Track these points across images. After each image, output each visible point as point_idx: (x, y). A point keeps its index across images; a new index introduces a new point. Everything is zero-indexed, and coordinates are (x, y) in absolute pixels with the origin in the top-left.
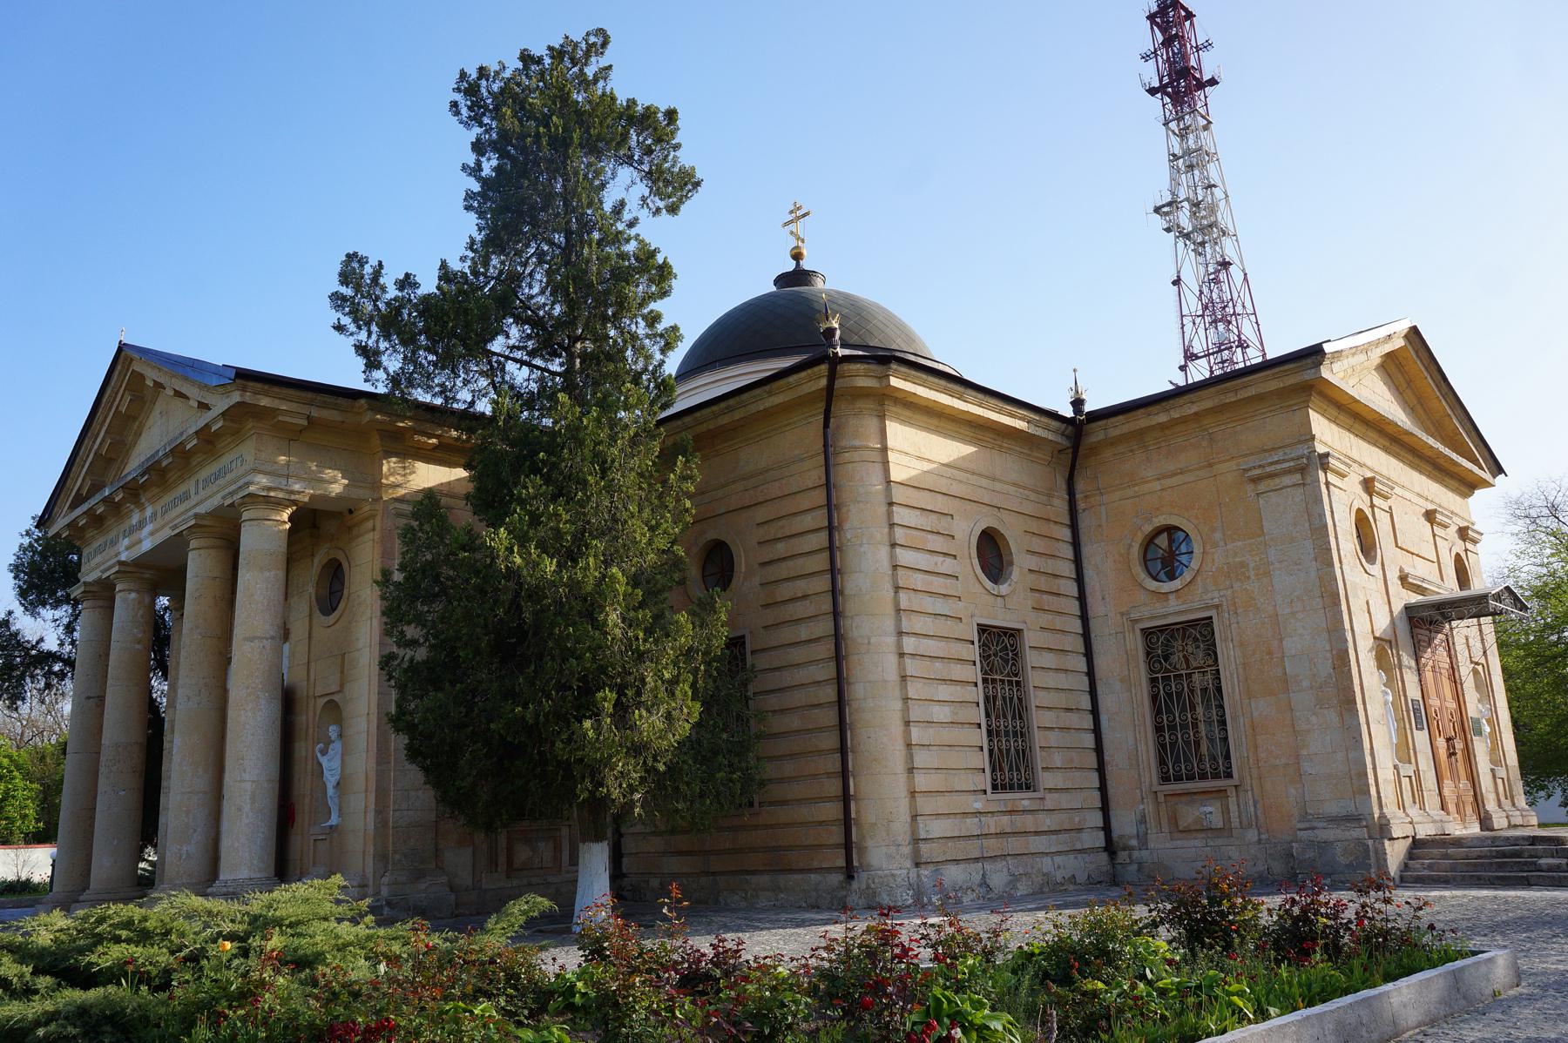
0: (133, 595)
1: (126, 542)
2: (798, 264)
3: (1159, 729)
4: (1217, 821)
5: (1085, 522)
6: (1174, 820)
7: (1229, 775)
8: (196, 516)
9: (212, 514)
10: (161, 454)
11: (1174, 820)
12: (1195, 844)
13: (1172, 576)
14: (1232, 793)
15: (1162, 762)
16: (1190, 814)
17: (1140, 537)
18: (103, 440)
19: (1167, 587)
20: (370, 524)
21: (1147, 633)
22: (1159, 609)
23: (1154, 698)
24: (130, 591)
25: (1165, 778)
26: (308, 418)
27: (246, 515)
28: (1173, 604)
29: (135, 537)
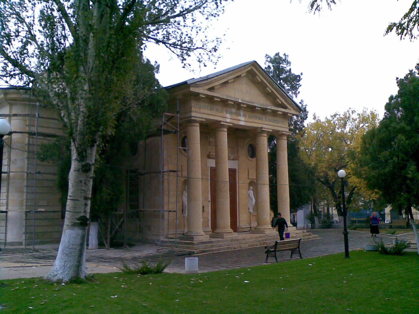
1: (228, 116)
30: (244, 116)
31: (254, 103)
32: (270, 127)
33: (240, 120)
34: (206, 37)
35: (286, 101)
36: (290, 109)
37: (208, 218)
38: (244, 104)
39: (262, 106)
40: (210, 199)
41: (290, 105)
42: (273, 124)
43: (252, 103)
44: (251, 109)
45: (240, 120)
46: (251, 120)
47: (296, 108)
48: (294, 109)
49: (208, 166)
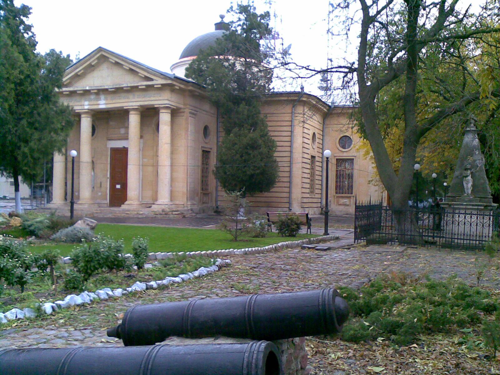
0: (89, 119)
1: (87, 103)
2: (222, 20)
3: (336, 182)
4: (348, 203)
5: (326, 130)
6: (338, 202)
7: (352, 193)
8: (138, 106)
9: (141, 106)
10: (124, 86)
11: (338, 202)
12: (341, 208)
13: (344, 148)
14: (352, 197)
15: (336, 189)
16: (342, 201)
17: (339, 137)
18: (80, 71)
19: (344, 150)
20: (182, 114)
21: (337, 159)
22: (341, 154)
23: (337, 175)
24: (88, 117)
25: (336, 193)
26: (180, 87)
27: (161, 111)
28: (345, 154)
29: (95, 103)
30: (106, 99)
31: (104, 86)
32: (134, 104)
33: (99, 104)
34: (232, 3)
35: (148, 73)
36: (155, 80)
37: (106, 192)
38: (93, 90)
39: (114, 87)
40: (109, 176)
41: (154, 75)
42: (143, 99)
43: (101, 86)
44: (118, 91)
45: (99, 104)
46: (114, 101)
47: (162, 76)
48: (162, 78)
49: (108, 146)
